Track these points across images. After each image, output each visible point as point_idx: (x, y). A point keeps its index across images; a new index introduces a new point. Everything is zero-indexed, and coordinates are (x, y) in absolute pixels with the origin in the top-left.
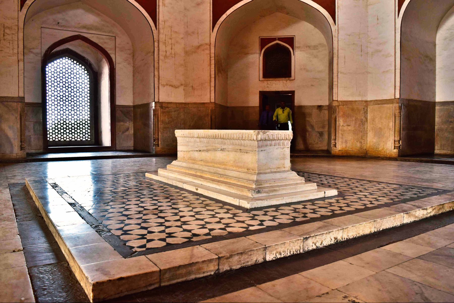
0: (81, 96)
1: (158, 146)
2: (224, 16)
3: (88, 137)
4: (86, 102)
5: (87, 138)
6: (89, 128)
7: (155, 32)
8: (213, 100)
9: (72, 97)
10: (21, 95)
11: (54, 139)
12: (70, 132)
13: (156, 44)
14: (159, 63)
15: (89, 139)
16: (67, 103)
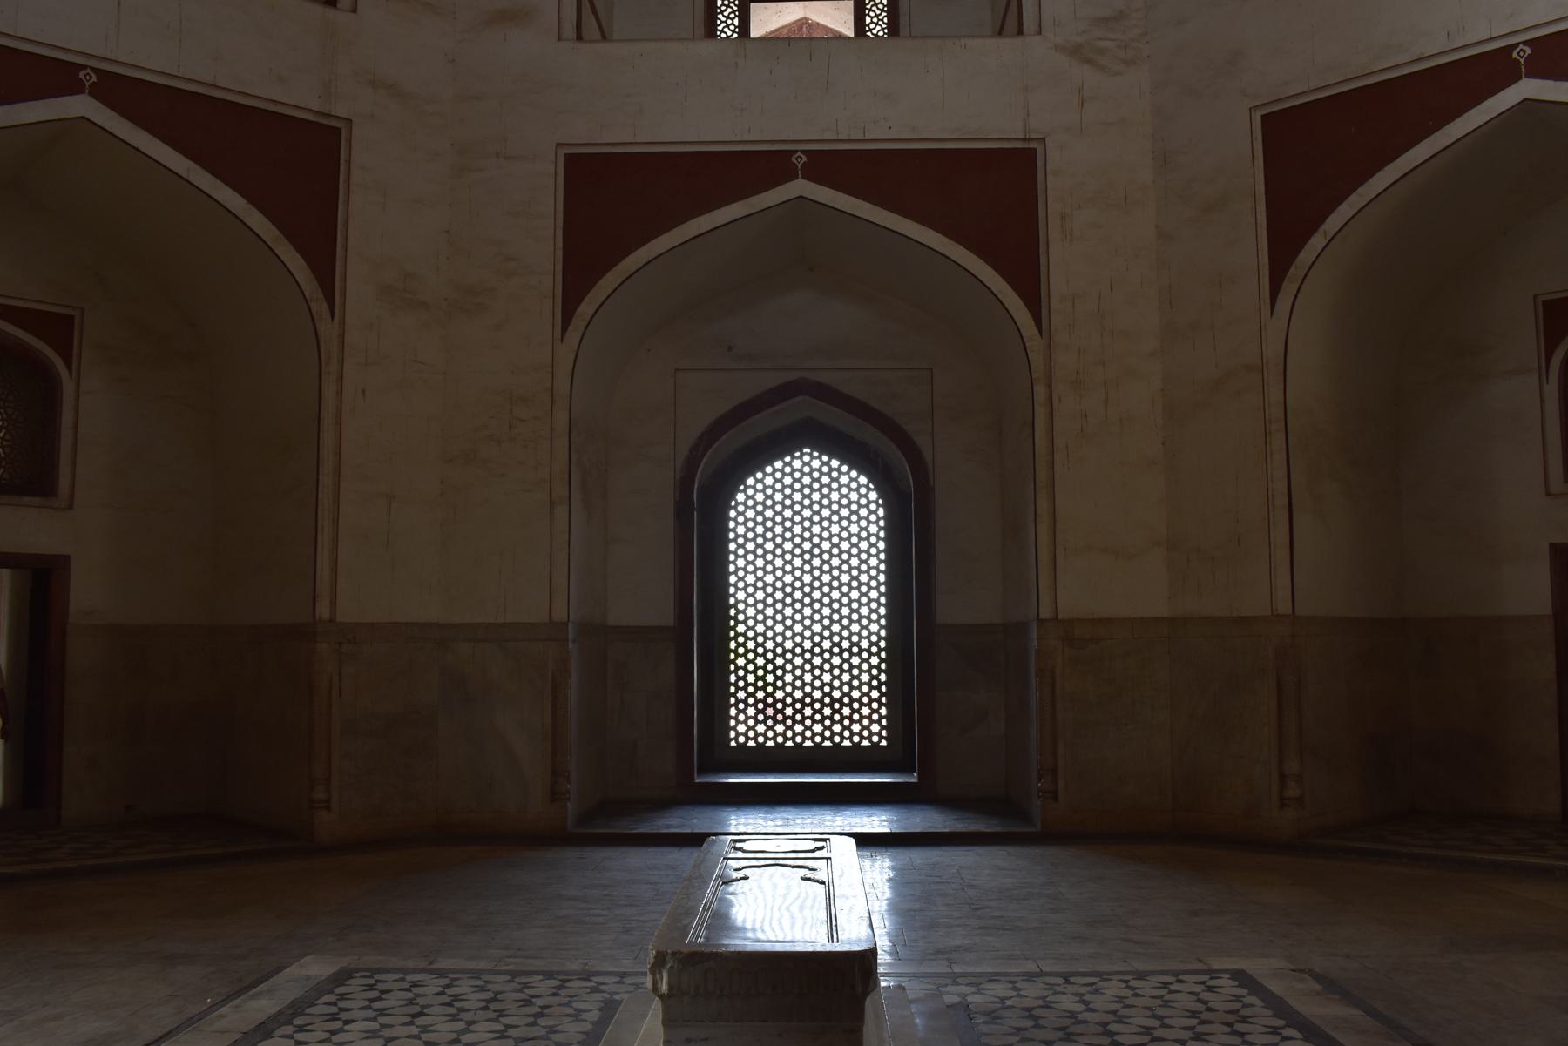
0: (854, 584)
1: (1056, 799)
2: (1317, 241)
3: (879, 734)
4: (874, 605)
5: (875, 739)
6: (884, 700)
7: (1035, 342)
8: (1284, 607)
9: (826, 589)
10: (560, 614)
11: (761, 739)
12: (818, 717)
13: (1040, 391)
14: (1052, 465)
15: (884, 743)
16: (807, 611)
